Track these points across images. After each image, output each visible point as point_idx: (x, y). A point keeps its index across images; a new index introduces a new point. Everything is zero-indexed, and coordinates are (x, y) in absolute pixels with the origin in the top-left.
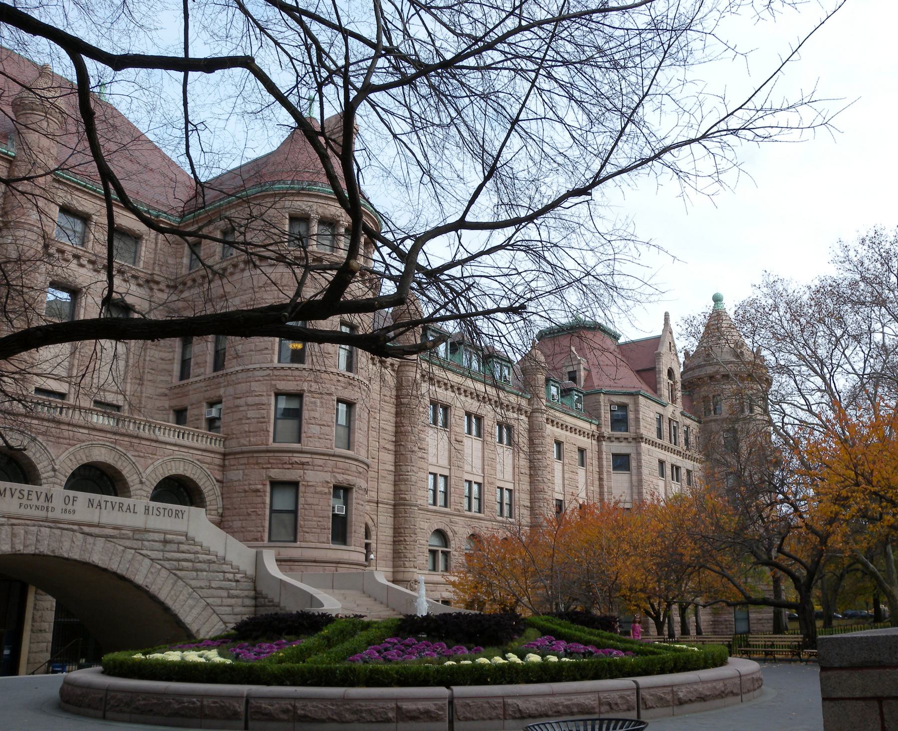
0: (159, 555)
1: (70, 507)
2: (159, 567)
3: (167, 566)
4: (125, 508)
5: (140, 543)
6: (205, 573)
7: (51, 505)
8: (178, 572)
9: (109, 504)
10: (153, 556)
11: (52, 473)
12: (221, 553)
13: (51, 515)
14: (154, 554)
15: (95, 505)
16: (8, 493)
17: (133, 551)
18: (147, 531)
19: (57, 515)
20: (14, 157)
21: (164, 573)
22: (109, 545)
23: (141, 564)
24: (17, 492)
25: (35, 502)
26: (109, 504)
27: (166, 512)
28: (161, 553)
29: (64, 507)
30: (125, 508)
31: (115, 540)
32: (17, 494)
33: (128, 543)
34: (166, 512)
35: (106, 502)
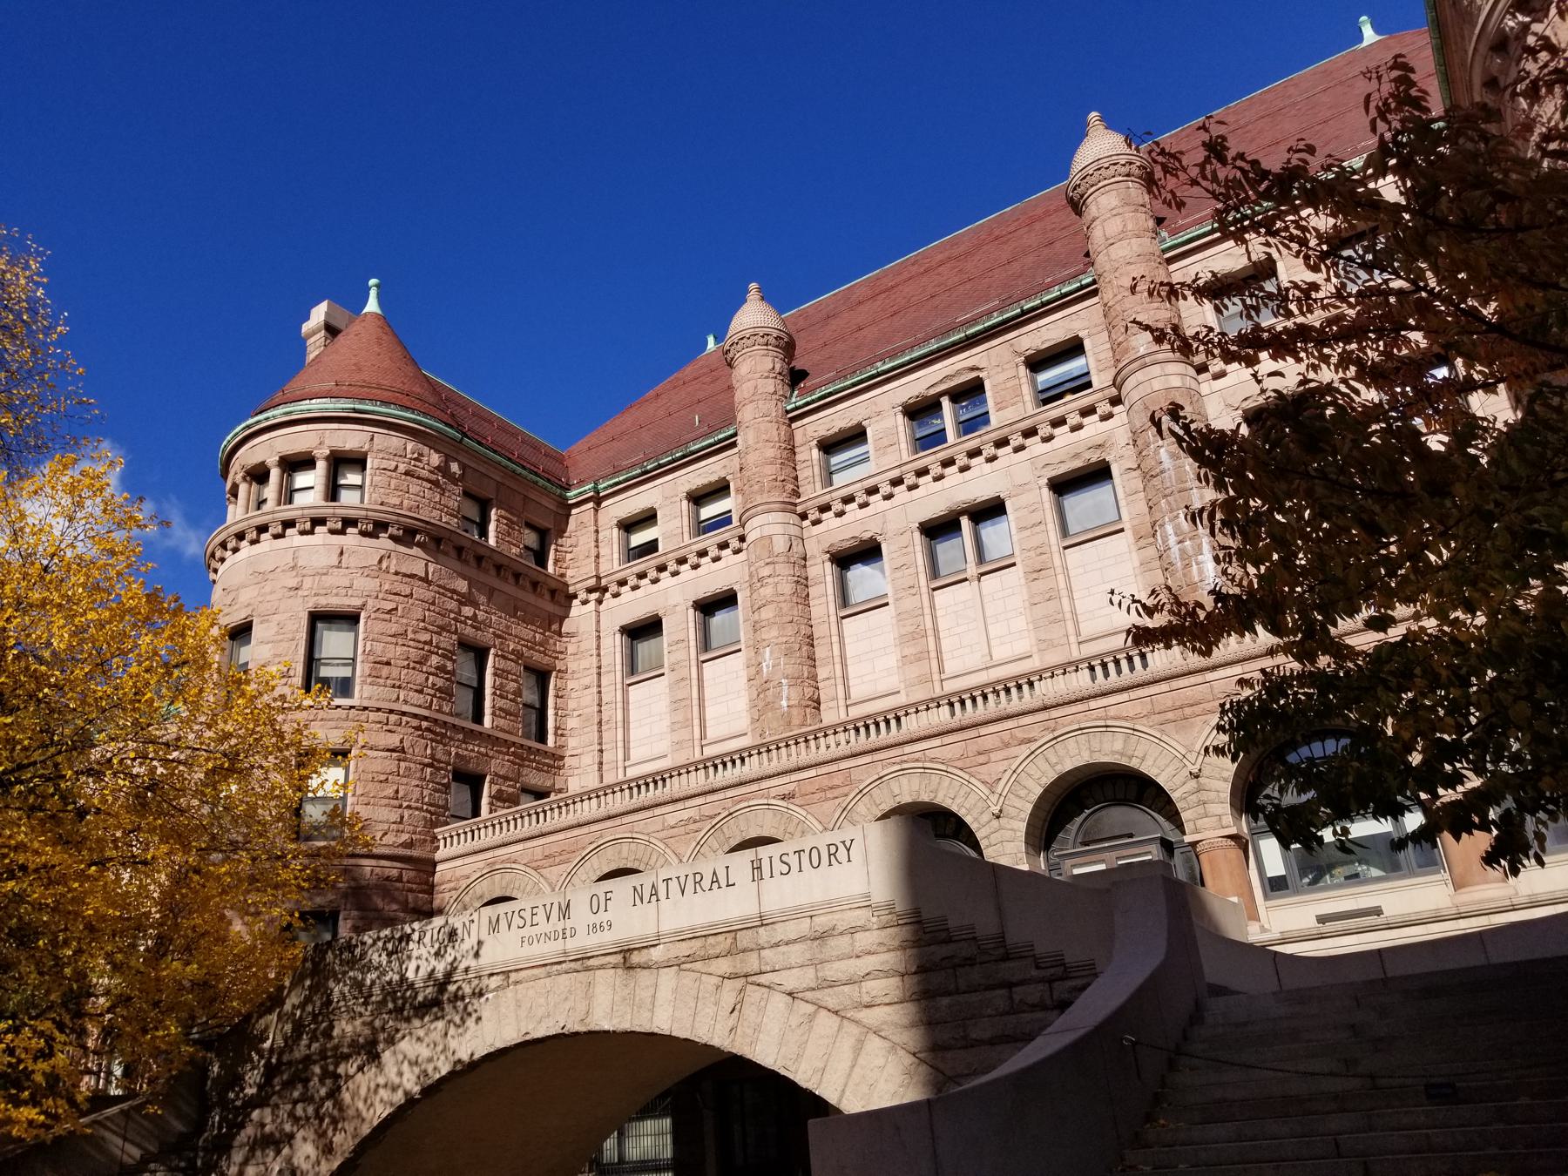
0: (806, 978)
1: (602, 917)
2: (810, 1008)
3: (831, 1002)
4: (706, 883)
5: (754, 955)
6: (945, 1001)
7: (569, 923)
8: (864, 1015)
9: (674, 885)
10: (789, 987)
11: (1193, 784)
12: (986, 925)
13: (572, 945)
14: (791, 980)
15: (646, 897)
16: (503, 923)
17: (739, 983)
18: (763, 922)
19: (583, 941)
20: (1094, 282)
21: (826, 1022)
22: (687, 979)
23: (762, 1010)
24: (516, 913)
25: (544, 927)
26: (674, 885)
27: (804, 857)
28: (811, 972)
29: (596, 919)
30: (706, 883)
31: (698, 966)
32: (517, 921)
33: (724, 966)
34: (804, 857)
35: (667, 880)
